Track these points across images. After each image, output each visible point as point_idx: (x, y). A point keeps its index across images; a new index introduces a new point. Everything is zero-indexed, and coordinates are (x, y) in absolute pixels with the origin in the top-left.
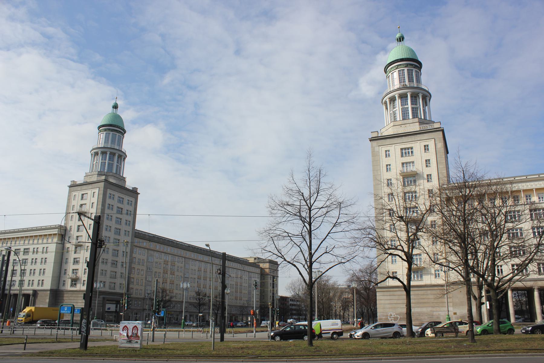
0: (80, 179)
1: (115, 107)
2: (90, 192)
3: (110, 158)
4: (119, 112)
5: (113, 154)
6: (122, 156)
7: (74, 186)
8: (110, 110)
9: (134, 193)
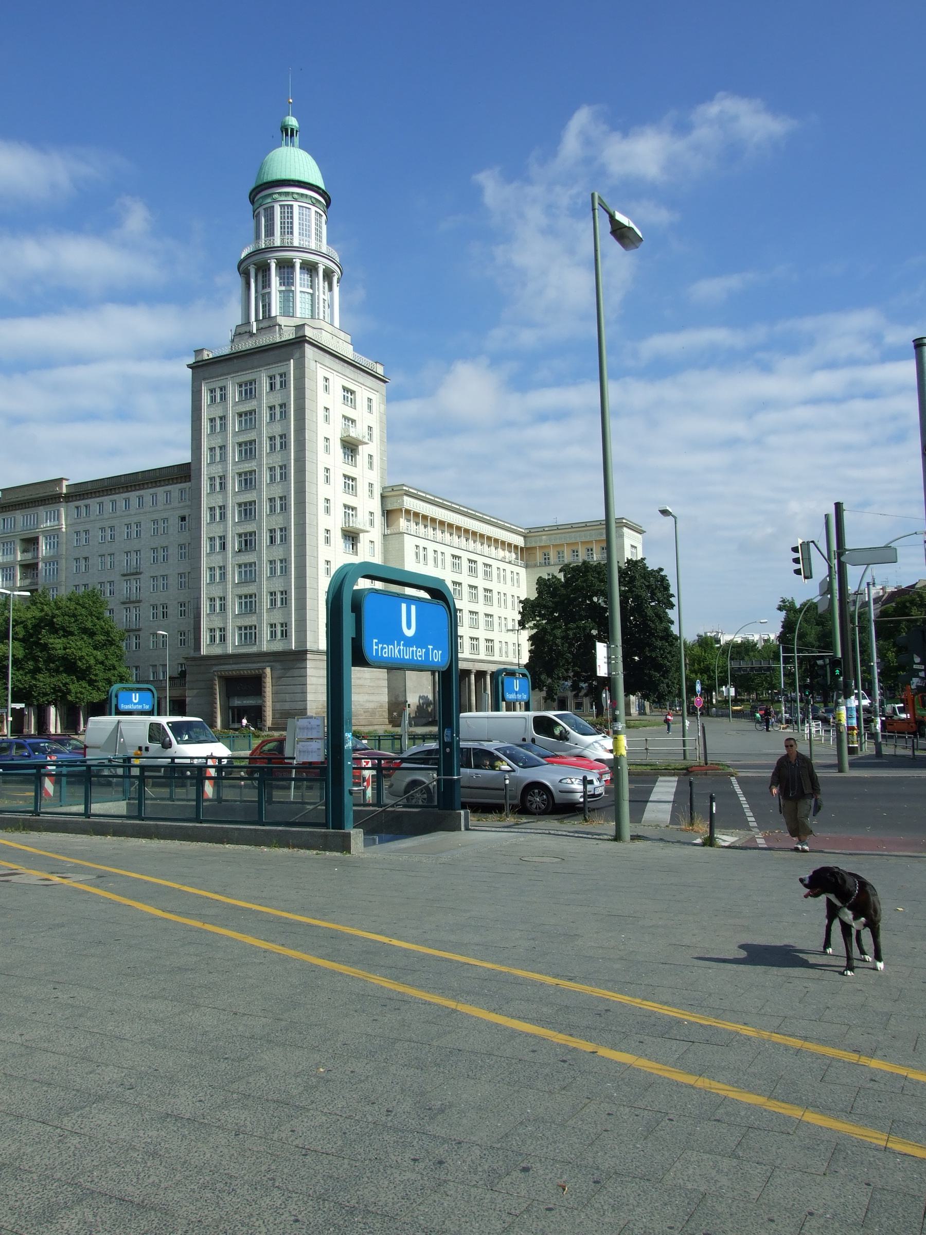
7: (203, 368)
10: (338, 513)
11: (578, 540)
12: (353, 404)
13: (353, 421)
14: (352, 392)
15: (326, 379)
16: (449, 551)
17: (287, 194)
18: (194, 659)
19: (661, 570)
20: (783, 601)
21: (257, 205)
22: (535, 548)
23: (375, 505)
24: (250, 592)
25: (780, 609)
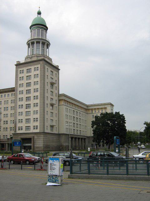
0: (22, 60)
1: (39, 13)
2: (32, 68)
3: (42, 46)
4: (42, 16)
5: (43, 44)
6: (48, 45)
7: (18, 65)
8: (36, 16)
9: (57, 69)
10: (49, 99)
11: (100, 108)
12: (52, 75)
13: (53, 79)
14: (53, 72)
15: (47, 69)
16: (72, 110)
17: (39, 27)
18: (14, 134)
19: (123, 115)
20: (145, 122)
21: (31, 29)
22: (89, 109)
23: (57, 98)
24: (29, 118)
25: (144, 124)
